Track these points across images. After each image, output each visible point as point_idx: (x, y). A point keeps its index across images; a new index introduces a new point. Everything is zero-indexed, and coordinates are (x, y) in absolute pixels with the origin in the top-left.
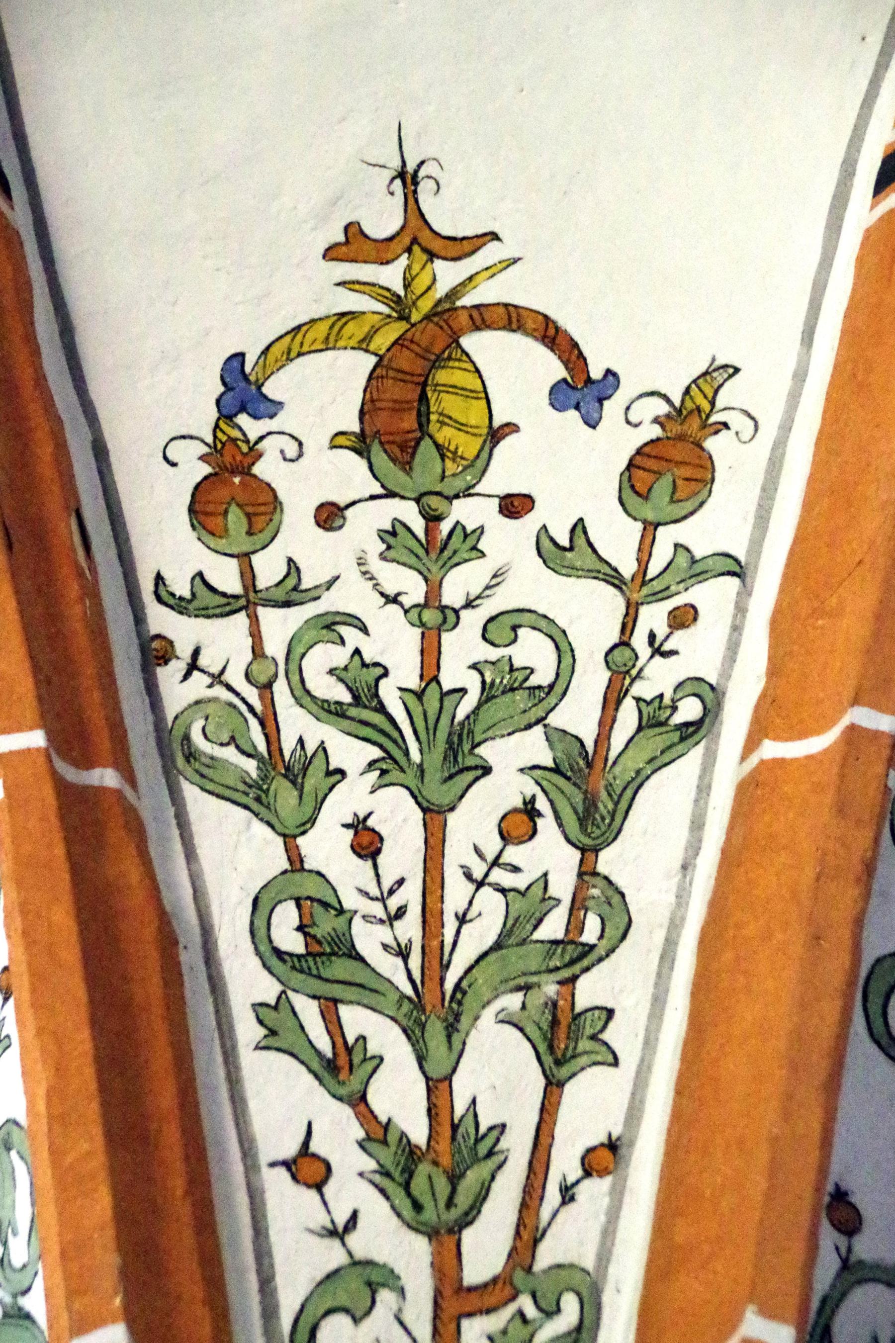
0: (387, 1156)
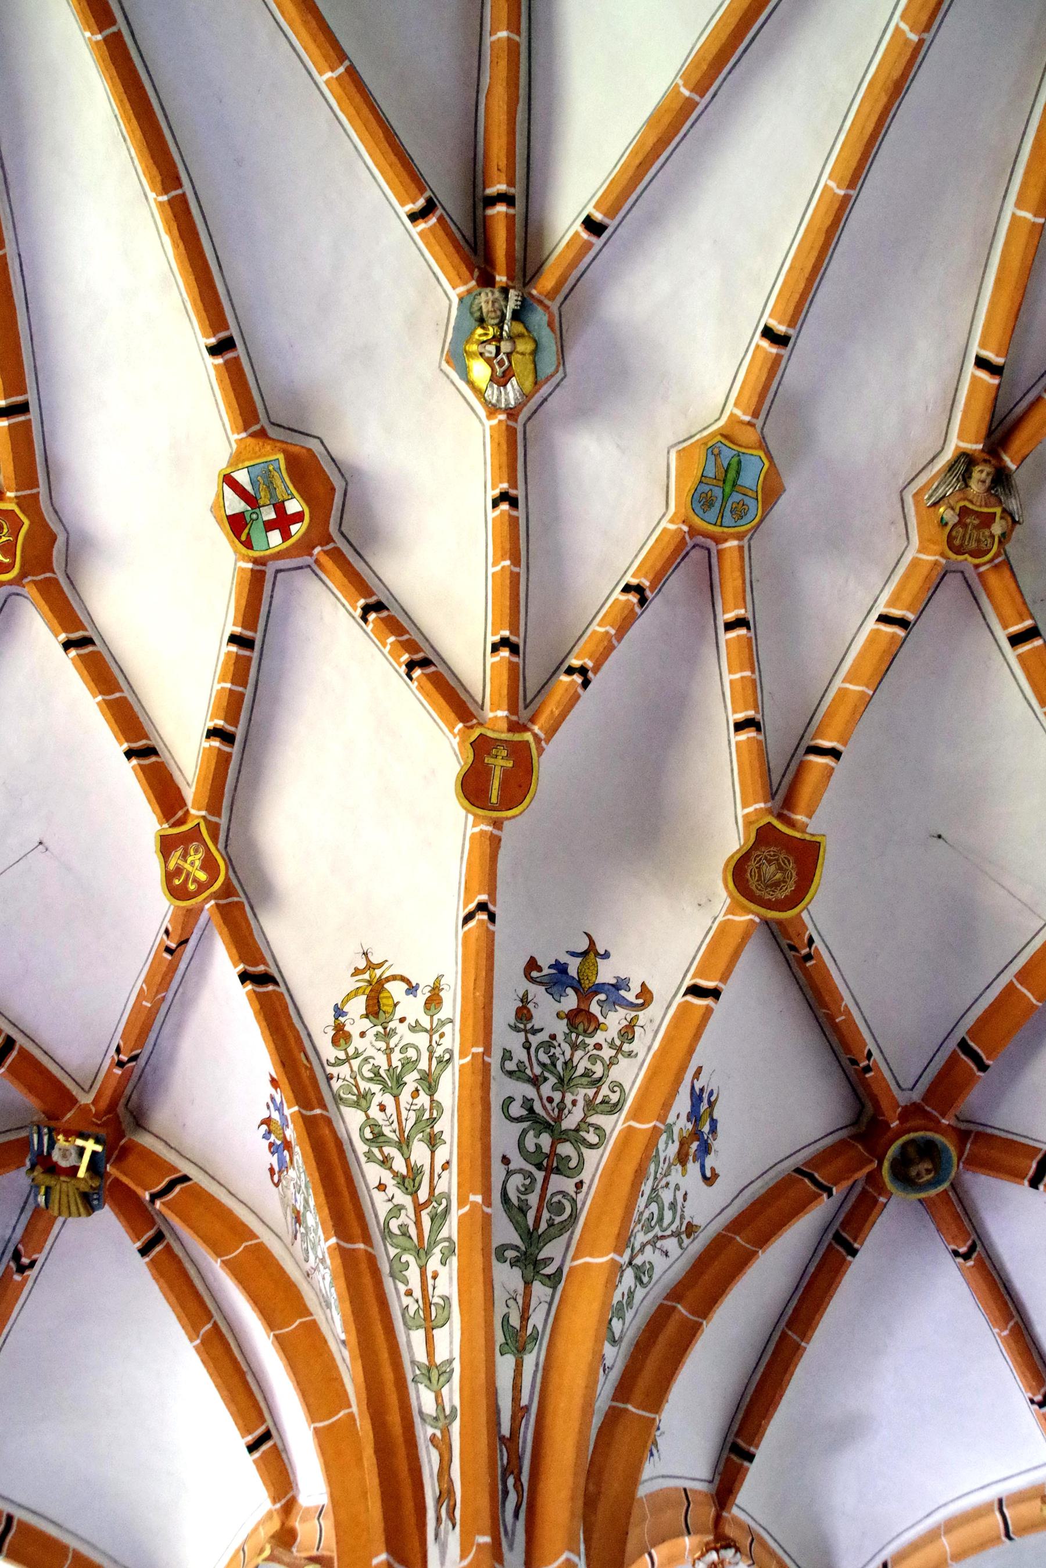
0: (398, 1179)
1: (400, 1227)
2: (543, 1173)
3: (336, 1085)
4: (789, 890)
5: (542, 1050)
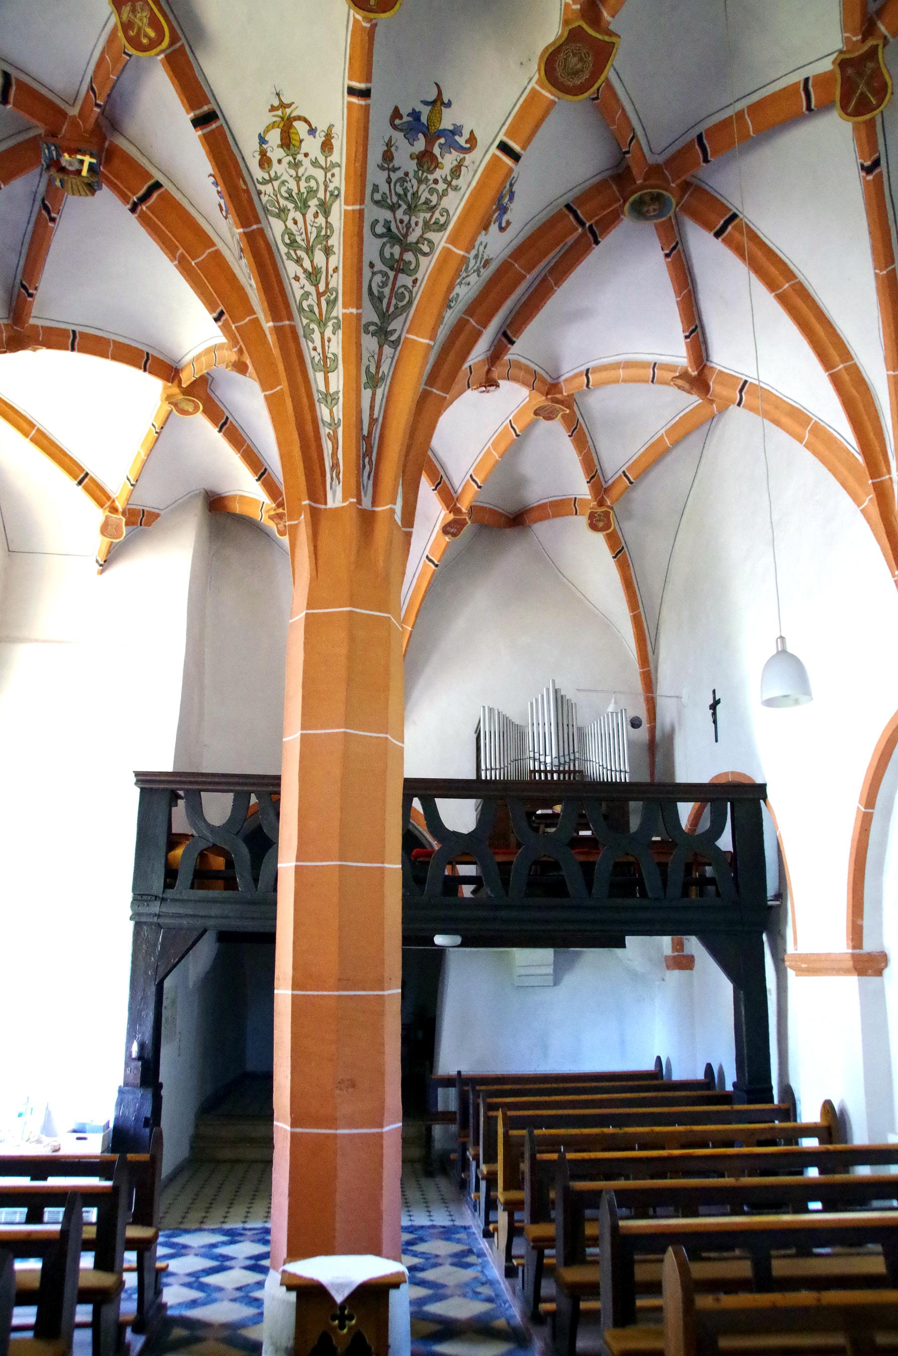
1: (309, 306)
2: (394, 273)
3: (264, 199)
4: (584, 78)
5: (398, 184)
